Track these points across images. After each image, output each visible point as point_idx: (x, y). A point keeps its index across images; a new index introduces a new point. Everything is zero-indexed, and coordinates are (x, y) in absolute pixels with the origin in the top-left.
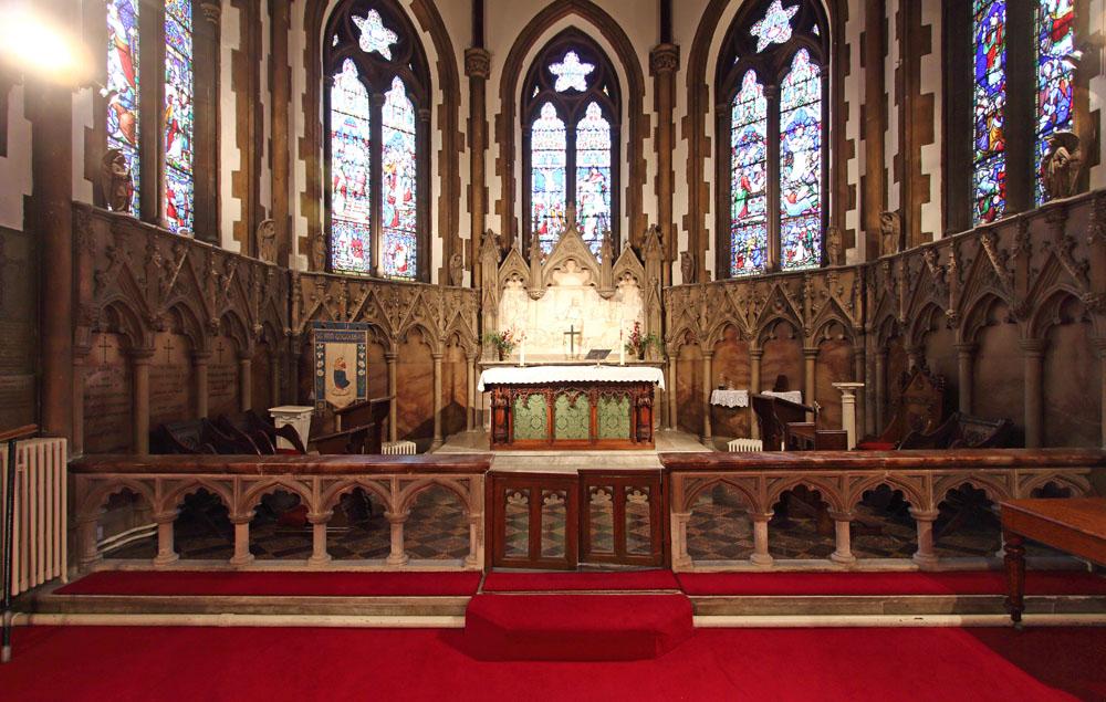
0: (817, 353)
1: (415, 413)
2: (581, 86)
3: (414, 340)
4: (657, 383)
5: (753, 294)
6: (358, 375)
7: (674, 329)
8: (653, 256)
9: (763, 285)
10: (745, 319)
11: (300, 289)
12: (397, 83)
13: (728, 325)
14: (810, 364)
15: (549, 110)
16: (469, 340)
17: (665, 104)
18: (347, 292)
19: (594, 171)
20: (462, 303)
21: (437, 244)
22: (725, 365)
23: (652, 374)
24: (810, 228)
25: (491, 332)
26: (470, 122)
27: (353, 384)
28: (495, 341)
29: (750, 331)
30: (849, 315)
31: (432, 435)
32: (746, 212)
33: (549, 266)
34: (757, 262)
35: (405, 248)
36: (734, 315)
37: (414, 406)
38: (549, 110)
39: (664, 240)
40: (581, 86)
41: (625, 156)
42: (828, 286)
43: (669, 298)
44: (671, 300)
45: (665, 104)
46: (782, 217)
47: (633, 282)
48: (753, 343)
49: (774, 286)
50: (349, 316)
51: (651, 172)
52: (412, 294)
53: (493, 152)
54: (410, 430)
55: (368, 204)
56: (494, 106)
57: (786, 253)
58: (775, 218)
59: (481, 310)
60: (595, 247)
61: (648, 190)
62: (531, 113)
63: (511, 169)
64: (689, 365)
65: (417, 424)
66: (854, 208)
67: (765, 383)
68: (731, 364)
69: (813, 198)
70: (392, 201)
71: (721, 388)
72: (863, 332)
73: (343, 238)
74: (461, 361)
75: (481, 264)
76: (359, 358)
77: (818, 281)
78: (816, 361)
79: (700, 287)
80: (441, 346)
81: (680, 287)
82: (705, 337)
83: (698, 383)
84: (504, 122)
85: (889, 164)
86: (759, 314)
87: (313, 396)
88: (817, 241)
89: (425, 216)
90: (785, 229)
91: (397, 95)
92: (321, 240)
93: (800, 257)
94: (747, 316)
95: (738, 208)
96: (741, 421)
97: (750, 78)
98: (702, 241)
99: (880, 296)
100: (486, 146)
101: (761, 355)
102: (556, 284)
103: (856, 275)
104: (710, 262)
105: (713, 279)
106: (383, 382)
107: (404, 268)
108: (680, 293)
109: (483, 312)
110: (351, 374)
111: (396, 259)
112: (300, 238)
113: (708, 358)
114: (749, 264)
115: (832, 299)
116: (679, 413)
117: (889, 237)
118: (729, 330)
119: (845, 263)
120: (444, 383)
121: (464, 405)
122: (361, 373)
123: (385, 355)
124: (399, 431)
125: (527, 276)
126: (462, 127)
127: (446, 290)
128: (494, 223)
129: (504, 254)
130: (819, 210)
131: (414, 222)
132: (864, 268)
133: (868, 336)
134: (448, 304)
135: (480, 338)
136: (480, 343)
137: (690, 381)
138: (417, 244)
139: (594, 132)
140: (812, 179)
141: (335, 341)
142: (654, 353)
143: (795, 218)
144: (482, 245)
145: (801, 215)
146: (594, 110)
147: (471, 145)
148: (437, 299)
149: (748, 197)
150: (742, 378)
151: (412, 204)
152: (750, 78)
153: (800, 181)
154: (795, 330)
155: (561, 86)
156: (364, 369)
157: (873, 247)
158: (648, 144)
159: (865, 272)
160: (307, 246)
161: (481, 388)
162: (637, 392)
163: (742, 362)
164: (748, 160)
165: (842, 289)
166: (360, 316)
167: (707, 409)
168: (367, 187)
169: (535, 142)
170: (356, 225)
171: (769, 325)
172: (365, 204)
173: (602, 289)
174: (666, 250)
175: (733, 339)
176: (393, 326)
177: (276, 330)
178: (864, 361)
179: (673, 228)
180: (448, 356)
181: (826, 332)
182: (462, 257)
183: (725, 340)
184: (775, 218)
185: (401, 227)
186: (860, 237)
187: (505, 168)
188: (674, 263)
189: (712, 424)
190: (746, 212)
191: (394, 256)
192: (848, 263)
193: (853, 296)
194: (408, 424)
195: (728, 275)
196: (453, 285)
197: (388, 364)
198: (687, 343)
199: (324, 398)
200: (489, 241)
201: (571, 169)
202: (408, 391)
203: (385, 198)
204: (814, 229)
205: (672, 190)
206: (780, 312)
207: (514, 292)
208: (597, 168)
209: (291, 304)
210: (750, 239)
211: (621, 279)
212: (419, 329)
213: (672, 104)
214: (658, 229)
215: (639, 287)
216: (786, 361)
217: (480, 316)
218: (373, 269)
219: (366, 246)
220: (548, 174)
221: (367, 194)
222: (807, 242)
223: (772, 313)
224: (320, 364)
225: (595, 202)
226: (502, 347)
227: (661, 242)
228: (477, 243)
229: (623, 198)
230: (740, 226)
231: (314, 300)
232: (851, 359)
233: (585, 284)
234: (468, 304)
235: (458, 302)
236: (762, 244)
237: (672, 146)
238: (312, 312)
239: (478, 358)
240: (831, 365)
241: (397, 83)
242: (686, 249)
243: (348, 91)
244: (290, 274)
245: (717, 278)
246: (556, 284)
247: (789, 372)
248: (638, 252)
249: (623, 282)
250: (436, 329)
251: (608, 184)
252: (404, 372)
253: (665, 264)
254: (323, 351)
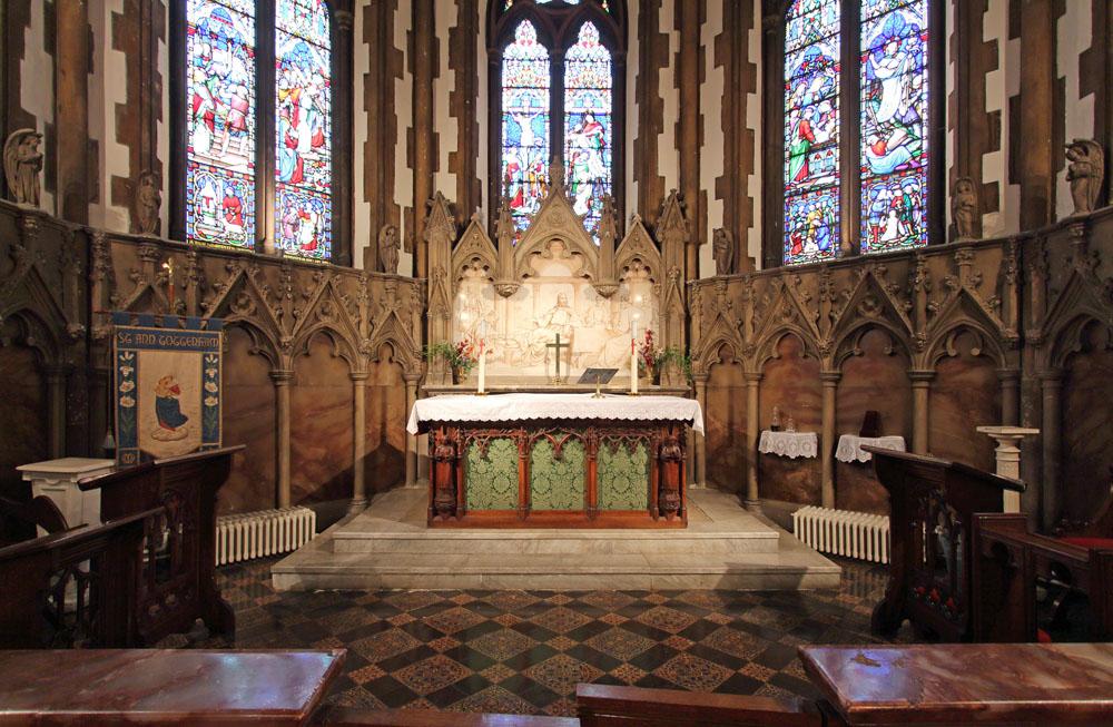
0: (933, 378)
1: (323, 462)
3: (322, 352)
4: (691, 423)
5: (827, 287)
6: (204, 407)
7: (703, 340)
8: (673, 235)
9: (845, 273)
10: (813, 325)
11: (109, 260)
13: (785, 334)
14: (921, 395)
15: (526, 31)
16: (409, 354)
18: (200, 271)
19: (589, 119)
20: (397, 299)
21: (362, 212)
22: (780, 394)
24: (908, 190)
25: (442, 343)
26: (413, 36)
27: (194, 423)
28: (447, 355)
29: (823, 343)
30: (994, 317)
31: (350, 493)
32: (806, 172)
33: (526, 247)
34: (824, 245)
35: (313, 216)
36: (796, 320)
37: (322, 452)
38: (526, 31)
39: (689, 212)
42: (956, 271)
43: (696, 296)
44: (700, 298)
46: (864, 176)
47: (643, 273)
48: (826, 362)
49: (862, 274)
50: (203, 310)
51: (670, 116)
52: (317, 281)
53: (446, 82)
54: (313, 488)
55: (252, 144)
57: (869, 228)
58: (853, 176)
59: (426, 310)
61: (666, 142)
62: (501, 36)
63: (472, 108)
64: (724, 394)
65: (326, 479)
66: (998, 149)
67: (845, 422)
68: (789, 393)
69: (914, 146)
70: (292, 144)
71: (775, 429)
72: (1021, 343)
73: (207, 194)
74: (397, 384)
75: (427, 243)
76: (205, 378)
77: (938, 266)
78: (930, 391)
79: (744, 278)
80: (363, 361)
81: (712, 281)
82: (750, 352)
83: (737, 419)
85: (1069, 70)
86: (837, 316)
87: (109, 442)
88: (920, 209)
89: (344, 170)
90: (867, 195)
94: (817, 321)
95: (794, 167)
96: (806, 478)
98: (743, 214)
99: (1059, 280)
100: (434, 73)
101: (838, 380)
102: (536, 275)
103: (1006, 252)
104: (754, 246)
105: (758, 267)
106: (269, 414)
107: (312, 246)
108: (711, 289)
109: (430, 314)
110: (189, 403)
112: (115, 179)
113: (756, 383)
114: (811, 248)
115: (963, 292)
116: (709, 463)
117: (1083, 182)
118: (786, 342)
119: (981, 236)
120: (369, 418)
121: (403, 450)
122: (210, 402)
123: (271, 374)
124: (294, 491)
125: (494, 262)
126: (400, 42)
127: (371, 277)
128: (447, 185)
129: (461, 230)
130: (924, 162)
131: (328, 179)
132: (1022, 242)
133: (1027, 353)
134: (376, 300)
135: (425, 350)
136: (424, 359)
137: (724, 416)
138: (334, 211)
139: (588, 64)
140: (912, 116)
141: (157, 347)
143: (884, 177)
144: (428, 215)
145: (895, 172)
146: (589, 32)
147: (413, 69)
148: (357, 290)
149: (810, 151)
150: (809, 415)
151: (326, 152)
153: (893, 121)
154: (894, 340)
156: (216, 395)
157: (1037, 205)
158: (666, 75)
159: (1024, 250)
160: (126, 192)
161: (412, 428)
162: (661, 436)
163: (805, 390)
165: (981, 278)
166: (224, 310)
167: (752, 459)
168: (250, 119)
169: (508, 74)
170: (231, 174)
171: (851, 336)
172: (247, 144)
173: (602, 281)
174: (691, 228)
175: (793, 356)
176: (284, 328)
177: (52, 327)
178: (1018, 391)
179: (702, 197)
180: (376, 376)
181: (949, 343)
182: (397, 230)
183: (779, 358)
184: (853, 176)
185: (307, 185)
186: (1009, 196)
187: (463, 105)
188: (702, 247)
189: (759, 482)
190: (806, 172)
191: (295, 226)
192: (986, 236)
193: (1000, 288)
194: (311, 479)
195: (779, 262)
196: (384, 271)
197: (276, 387)
198: (722, 362)
199: (136, 446)
200: (439, 208)
201: (557, 116)
202: (310, 429)
203: (280, 138)
204: (914, 192)
205: (699, 142)
206: (870, 314)
208: (593, 115)
209: (88, 285)
210: (812, 214)
211: (627, 269)
212: (328, 333)
213: (701, 17)
214: (681, 198)
215: (652, 280)
216: (880, 391)
217: (424, 319)
218: (260, 242)
219: (248, 208)
220: (525, 122)
221: (251, 129)
222: (904, 211)
223: (858, 315)
224: (127, 386)
225: (590, 164)
226: (457, 368)
227: (684, 216)
228: (422, 213)
230: (797, 193)
231: (135, 281)
232: (994, 387)
233: (576, 276)
234: (406, 301)
235: (391, 297)
236: (833, 218)
237: (700, 78)
238: (132, 299)
239: (421, 380)
240: (956, 397)
242: (720, 225)
244: (87, 235)
245: (764, 265)
246: (536, 275)
247: (882, 407)
248: (651, 231)
249: (630, 274)
250: (355, 336)
251: (608, 137)
252: (302, 397)
253: (691, 248)
254: (134, 363)
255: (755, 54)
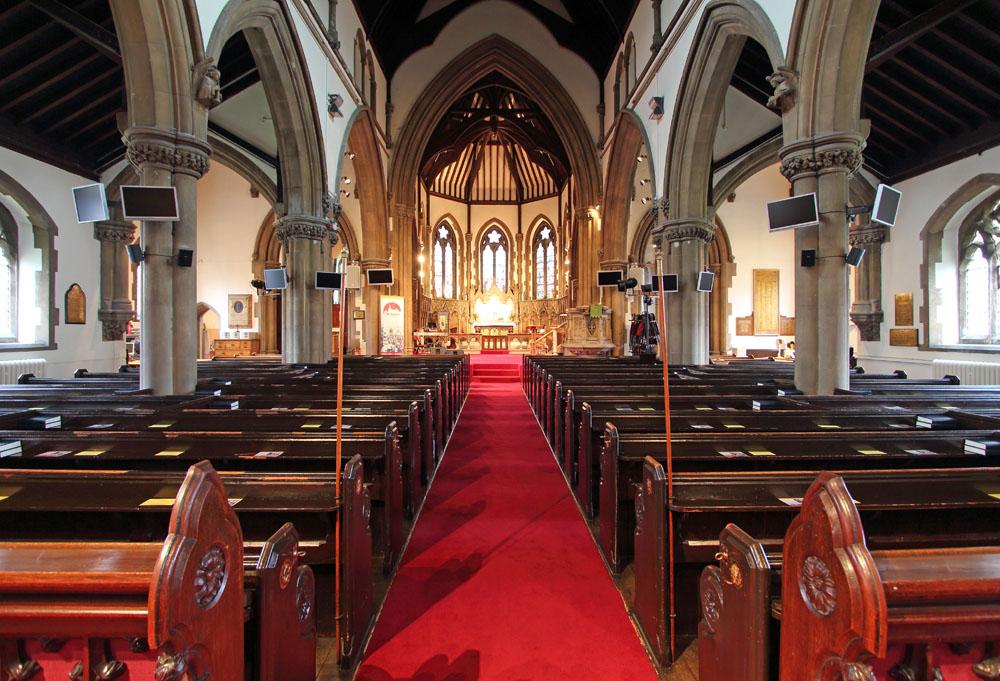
2: (497, 241)
12: (448, 244)
15: (488, 247)
17: (520, 249)
23: (513, 324)
38: (488, 247)
40: (497, 241)
41: (509, 263)
45: (520, 249)
51: (516, 268)
53: (473, 261)
56: (473, 248)
60: (501, 290)
61: (515, 274)
62: (483, 247)
84: (476, 253)
91: (448, 248)
92: (434, 291)
93: (550, 296)
97: (540, 245)
111: (449, 295)
128: (473, 282)
142: (517, 320)
146: (501, 248)
148: (459, 304)
152: (540, 245)
155: (491, 241)
158: (515, 260)
164: (540, 267)
165: (554, 304)
187: (476, 266)
201: (494, 265)
207: (479, 300)
210: (540, 289)
226: (475, 317)
229: (509, 276)
241: (448, 244)
243: (438, 246)
255: (531, 258)
